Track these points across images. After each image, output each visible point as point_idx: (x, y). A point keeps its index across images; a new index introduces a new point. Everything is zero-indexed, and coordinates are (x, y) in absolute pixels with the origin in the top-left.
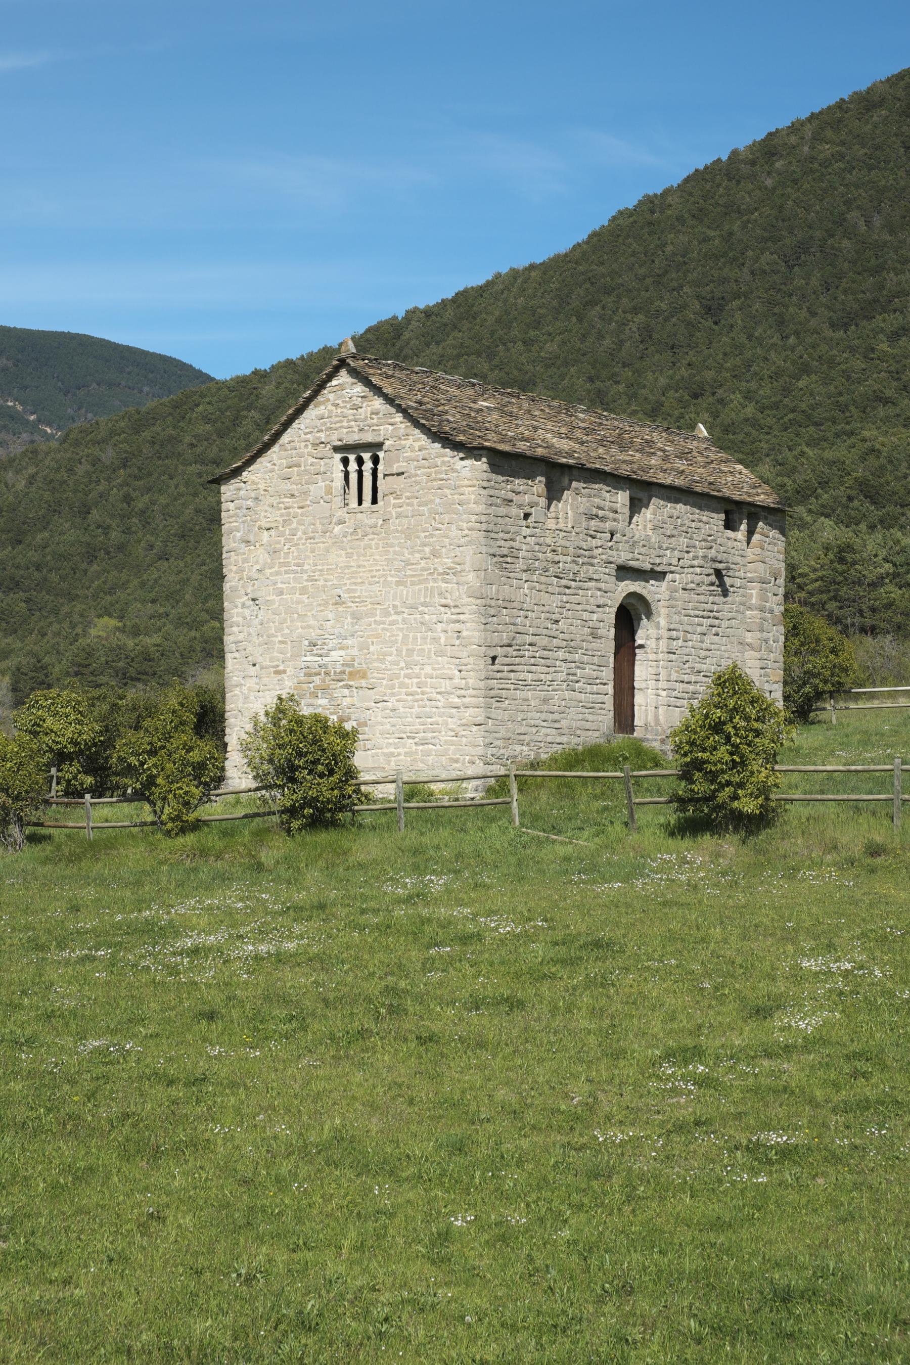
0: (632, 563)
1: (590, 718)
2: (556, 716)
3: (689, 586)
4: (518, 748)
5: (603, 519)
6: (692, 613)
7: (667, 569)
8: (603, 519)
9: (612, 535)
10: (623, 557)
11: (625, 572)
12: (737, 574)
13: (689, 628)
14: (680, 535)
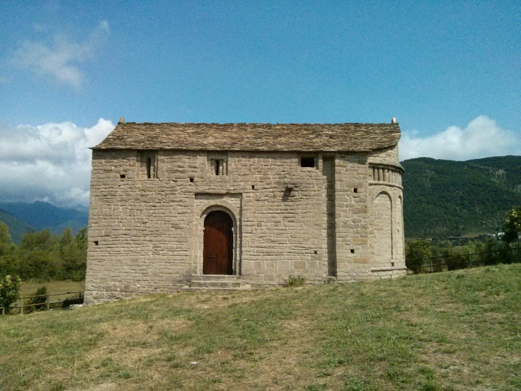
0: (207, 191)
7: (241, 191)
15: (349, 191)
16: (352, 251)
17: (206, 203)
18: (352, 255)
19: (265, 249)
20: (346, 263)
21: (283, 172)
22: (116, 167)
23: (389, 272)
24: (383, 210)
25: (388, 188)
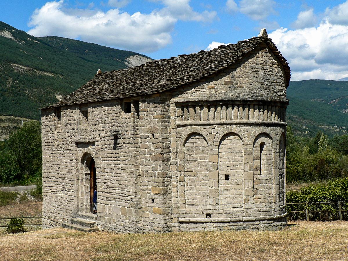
1: (70, 205)
2: (59, 204)
3: (104, 147)
4: (51, 214)
5: (70, 124)
6: (106, 159)
8: (70, 124)
9: (74, 130)
10: (77, 138)
11: (79, 144)
12: (127, 136)
13: (106, 167)
14: (99, 123)
15: (149, 137)
16: (153, 200)
17: (82, 151)
18: (152, 205)
19: (107, 194)
20: (149, 213)
21: (113, 120)
22: (49, 122)
23: (201, 224)
24: (196, 154)
25: (199, 127)
